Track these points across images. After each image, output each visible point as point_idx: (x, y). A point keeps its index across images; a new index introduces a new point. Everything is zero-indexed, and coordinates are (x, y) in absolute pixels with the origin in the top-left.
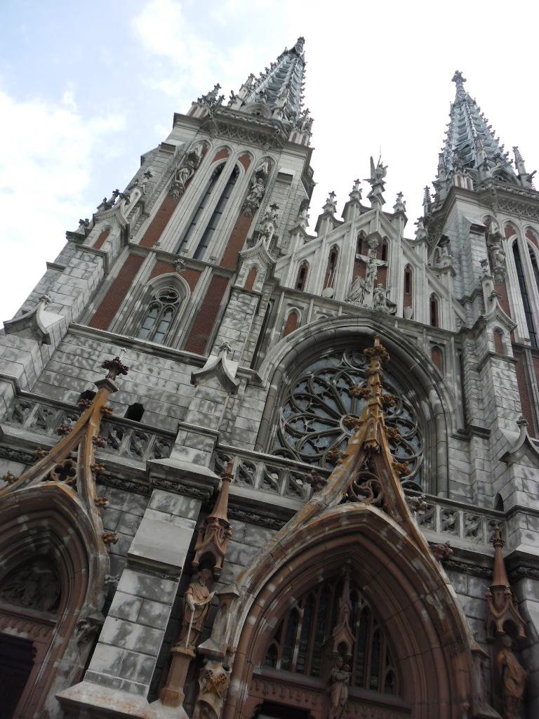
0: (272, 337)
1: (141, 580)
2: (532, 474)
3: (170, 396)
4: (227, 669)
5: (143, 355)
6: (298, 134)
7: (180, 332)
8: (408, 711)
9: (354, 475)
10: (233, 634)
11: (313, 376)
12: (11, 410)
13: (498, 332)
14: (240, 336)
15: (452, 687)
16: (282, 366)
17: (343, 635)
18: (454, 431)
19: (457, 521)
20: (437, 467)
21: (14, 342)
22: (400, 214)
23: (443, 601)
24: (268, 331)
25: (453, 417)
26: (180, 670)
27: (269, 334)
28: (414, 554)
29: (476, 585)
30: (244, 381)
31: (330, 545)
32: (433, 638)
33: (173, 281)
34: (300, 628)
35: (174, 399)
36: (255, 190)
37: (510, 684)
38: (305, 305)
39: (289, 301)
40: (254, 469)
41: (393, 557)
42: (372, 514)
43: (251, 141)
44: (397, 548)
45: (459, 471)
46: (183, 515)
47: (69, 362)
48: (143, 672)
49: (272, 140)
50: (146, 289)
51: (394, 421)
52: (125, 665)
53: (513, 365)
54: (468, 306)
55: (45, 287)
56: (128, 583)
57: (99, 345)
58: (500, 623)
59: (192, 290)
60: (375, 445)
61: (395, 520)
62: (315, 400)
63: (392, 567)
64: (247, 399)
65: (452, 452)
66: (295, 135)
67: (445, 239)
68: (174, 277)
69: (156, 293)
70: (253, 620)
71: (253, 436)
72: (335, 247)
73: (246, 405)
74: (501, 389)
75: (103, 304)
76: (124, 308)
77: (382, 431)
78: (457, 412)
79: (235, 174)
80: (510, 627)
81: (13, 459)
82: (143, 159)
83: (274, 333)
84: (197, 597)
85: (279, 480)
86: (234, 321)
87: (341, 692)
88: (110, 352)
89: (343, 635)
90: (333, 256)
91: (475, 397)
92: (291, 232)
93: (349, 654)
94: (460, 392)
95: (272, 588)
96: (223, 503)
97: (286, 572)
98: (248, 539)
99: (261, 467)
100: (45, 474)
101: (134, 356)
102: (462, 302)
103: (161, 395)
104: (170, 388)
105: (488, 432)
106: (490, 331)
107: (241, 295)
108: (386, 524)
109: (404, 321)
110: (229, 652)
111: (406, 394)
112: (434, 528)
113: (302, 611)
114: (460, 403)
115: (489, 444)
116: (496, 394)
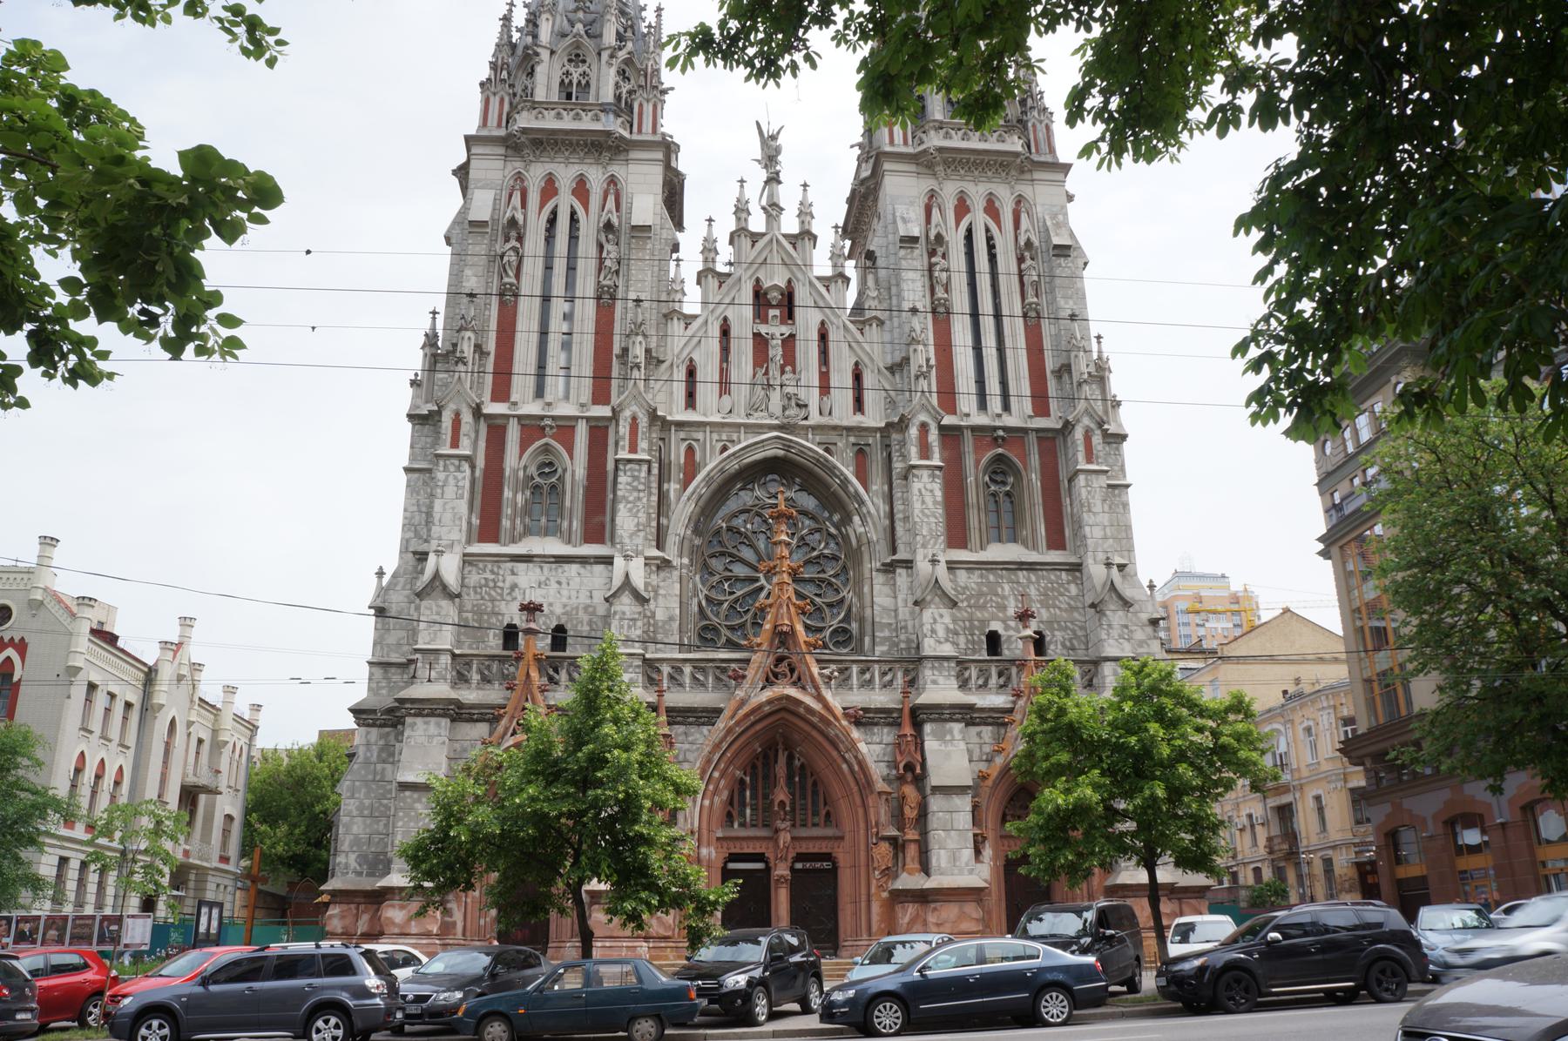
0: (672, 495)
2: (941, 616)
3: (586, 608)
5: (546, 566)
6: (645, 104)
7: (575, 524)
8: (842, 838)
9: (771, 659)
10: (692, 818)
11: (724, 525)
12: (454, 673)
13: (924, 427)
14: (638, 524)
15: (867, 821)
16: (689, 532)
17: (781, 795)
18: (878, 564)
19: (872, 676)
20: (862, 607)
21: (431, 609)
22: (806, 236)
23: (856, 757)
24: (666, 486)
25: (877, 548)
27: (668, 490)
28: (829, 723)
29: (888, 734)
30: (654, 568)
31: (758, 727)
32: (852, 784)
33: (547, 449)
34: (748, 793)
35: (591, 609)
36: (608, 263)
37: (907, 810)
38: (700, 436)
39: (682, 435)
40: (682, 671)
41: (814, 726)
42: (788, 698)
43: (582, 154)
44: (815, 720)
45: (884, 609)
47: (478, 597)
49: (609, 148)
50: (521, 473)
51: (818, 557)
53: (937, 473)
54: (897, 376)
55: (414, 501)
57: (499, 567)
59: (571, 458)
60: (785, 629)
61: (811, 695)
62: (731, 555)
63: (815, 733)
64: (662, 584)
65: (876, 588)
66: (641, 105)
67: (870, 256)
68: (547, 444)
69: (533, 470)
70: (707, 802)
71: (676, 625)
72: (725, 319)
73: (662, 592)
74: (922, 511)
75: (483, 510)
76: (507, 511)
77: (792, 609)
78: (882, 542)
79: (574, 219)
80: (909, 767)
81: (477, 721)
82: (448, 240)
83: (673, 487)
85: (706, 678)
86: (629, 506)
87: (785, 838)
88: (513, 573)
89: (781, 795)
90: (725, 332)
92: (665, 316)
93: (788, 808)
94: (887, 508)
95: (716, 774)
97: (725, 759)
98: (690, 739)
99: (687, 669)
100: (511, 731)
101: (538, 570)
102: (892, 369)
103: (577, 608)
104: (583, 599)
105: (911, 562)
106: (914, 431)
107: (628, 467)
108: (802, 702)
109: (816, 428)
110: (692, 833)
111: (830, 519)
112: (851, 689)
113: (748, 779)
114: (887, 522)
115: (911, 575)
116: (917, 519)
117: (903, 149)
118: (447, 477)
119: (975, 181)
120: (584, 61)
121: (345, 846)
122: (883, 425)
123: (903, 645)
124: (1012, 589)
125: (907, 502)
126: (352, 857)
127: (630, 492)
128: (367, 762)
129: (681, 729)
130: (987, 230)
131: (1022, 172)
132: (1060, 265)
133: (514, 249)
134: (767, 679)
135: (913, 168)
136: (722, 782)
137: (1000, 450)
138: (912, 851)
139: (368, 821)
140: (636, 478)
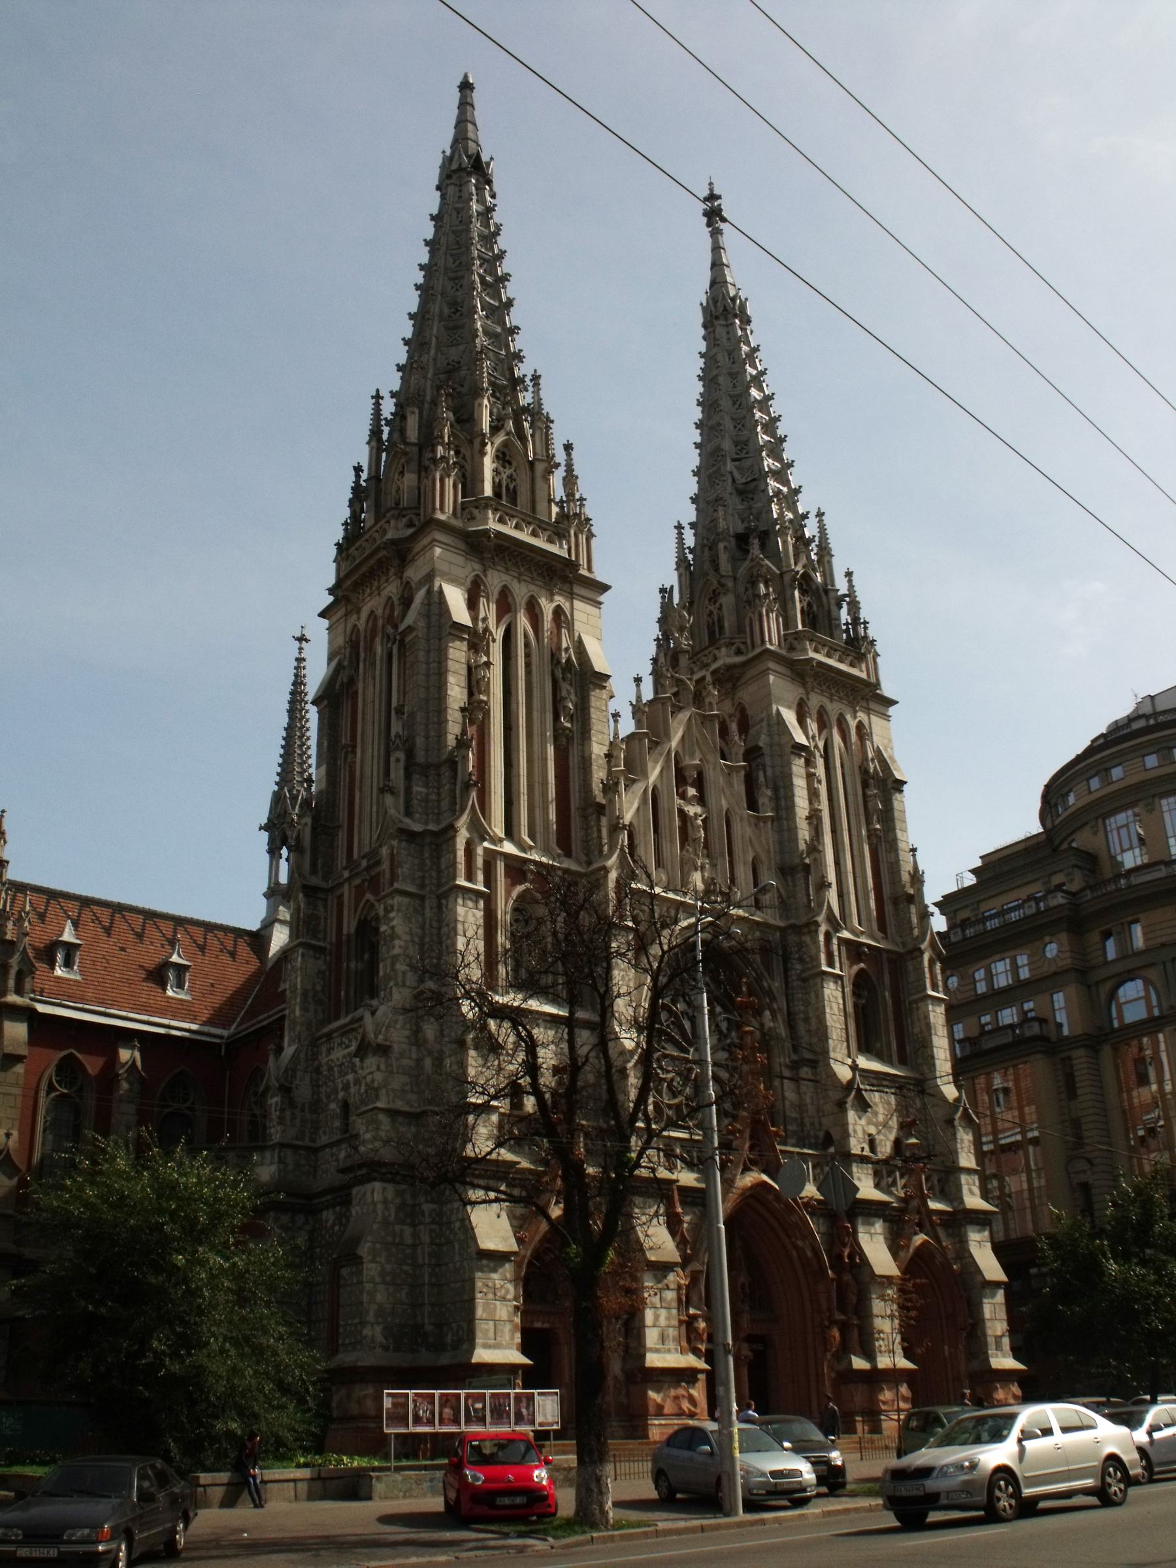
18: (787, 1060)
42: (764, 1184)
51: (729, 1045)
52: (663, 1338)
58: (846, 1254)
91: (802, 1016)
117: (778, 650)
118: (466, 912)
120: (510, 463)
121: (371, 1317)
122: (781, 924)
123: (813, 1141)
124: (881, 1097)
125: (807, 1003)
126: (378, 1329)
128: (385, 1223)
134: (745, 1163)
137: (862, 965)
138: (855, 1334)
139: (391, 1289)
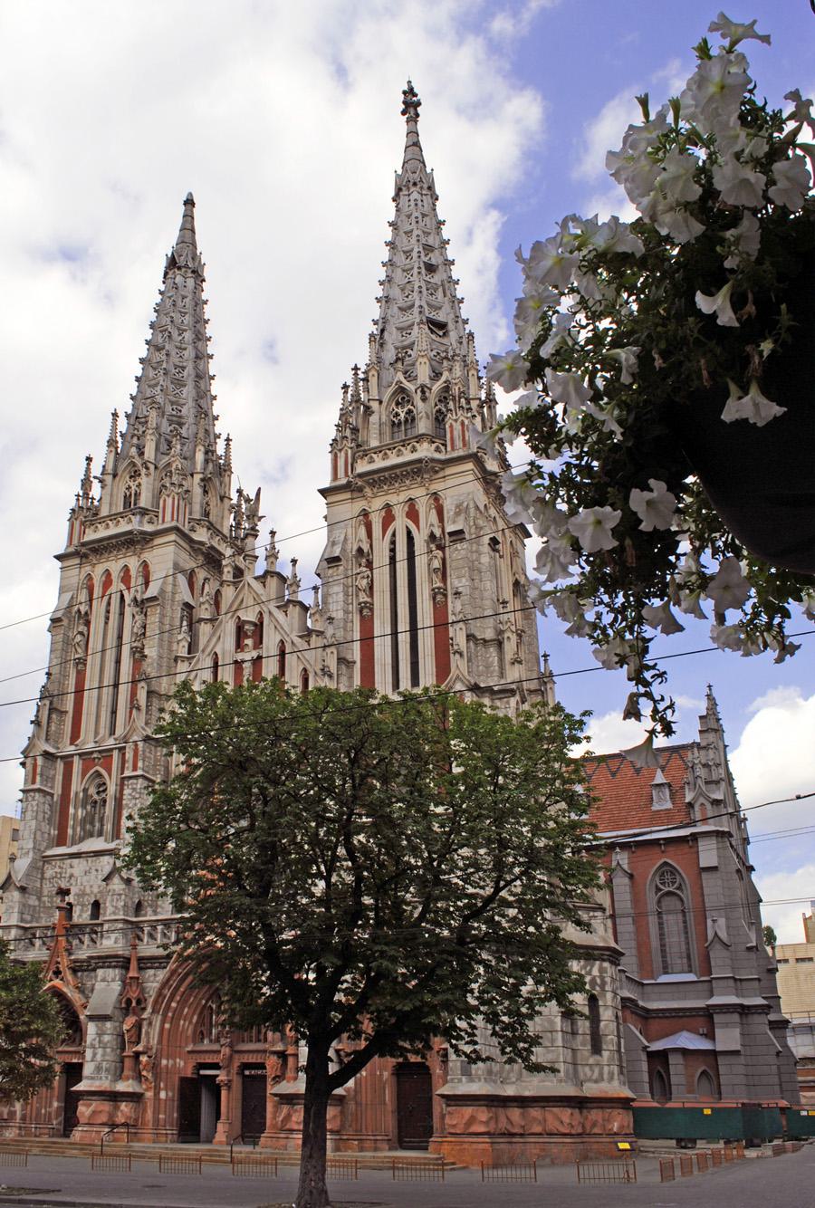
1: (97, 1026)
4: (149, 1057)
5: (90, 859)
26: (128, 1062)
33: (99, 775)
36: (135, 630)
46: (113, 980)
48: (106, 1070)
50: (81, 794)
52: (98, 1069)
56: (91, 1029)
59: (110, 775)
69: (92, 791)
70: (167, 1026)
72: (216, 654)
76: (71, 823)
84: (129, 1022)
88: (71, 867)
96: (134, 964)
97: (179, 993)
113: (214, 1006)
119: (398, 492)
127: (130, 800)
129: (151, 972)
130: (409, 533)
131: (437, 472)
132: (456, 549)
133: (81, 633)
135: (348, 495)
136: (186, 1010)
140: (134, 789)
